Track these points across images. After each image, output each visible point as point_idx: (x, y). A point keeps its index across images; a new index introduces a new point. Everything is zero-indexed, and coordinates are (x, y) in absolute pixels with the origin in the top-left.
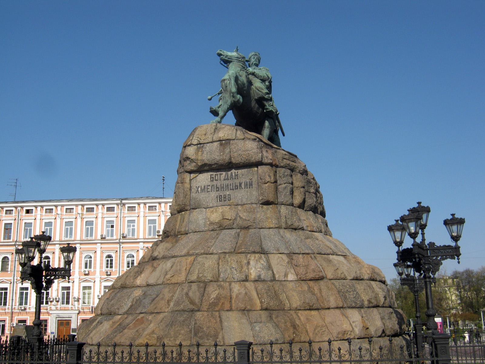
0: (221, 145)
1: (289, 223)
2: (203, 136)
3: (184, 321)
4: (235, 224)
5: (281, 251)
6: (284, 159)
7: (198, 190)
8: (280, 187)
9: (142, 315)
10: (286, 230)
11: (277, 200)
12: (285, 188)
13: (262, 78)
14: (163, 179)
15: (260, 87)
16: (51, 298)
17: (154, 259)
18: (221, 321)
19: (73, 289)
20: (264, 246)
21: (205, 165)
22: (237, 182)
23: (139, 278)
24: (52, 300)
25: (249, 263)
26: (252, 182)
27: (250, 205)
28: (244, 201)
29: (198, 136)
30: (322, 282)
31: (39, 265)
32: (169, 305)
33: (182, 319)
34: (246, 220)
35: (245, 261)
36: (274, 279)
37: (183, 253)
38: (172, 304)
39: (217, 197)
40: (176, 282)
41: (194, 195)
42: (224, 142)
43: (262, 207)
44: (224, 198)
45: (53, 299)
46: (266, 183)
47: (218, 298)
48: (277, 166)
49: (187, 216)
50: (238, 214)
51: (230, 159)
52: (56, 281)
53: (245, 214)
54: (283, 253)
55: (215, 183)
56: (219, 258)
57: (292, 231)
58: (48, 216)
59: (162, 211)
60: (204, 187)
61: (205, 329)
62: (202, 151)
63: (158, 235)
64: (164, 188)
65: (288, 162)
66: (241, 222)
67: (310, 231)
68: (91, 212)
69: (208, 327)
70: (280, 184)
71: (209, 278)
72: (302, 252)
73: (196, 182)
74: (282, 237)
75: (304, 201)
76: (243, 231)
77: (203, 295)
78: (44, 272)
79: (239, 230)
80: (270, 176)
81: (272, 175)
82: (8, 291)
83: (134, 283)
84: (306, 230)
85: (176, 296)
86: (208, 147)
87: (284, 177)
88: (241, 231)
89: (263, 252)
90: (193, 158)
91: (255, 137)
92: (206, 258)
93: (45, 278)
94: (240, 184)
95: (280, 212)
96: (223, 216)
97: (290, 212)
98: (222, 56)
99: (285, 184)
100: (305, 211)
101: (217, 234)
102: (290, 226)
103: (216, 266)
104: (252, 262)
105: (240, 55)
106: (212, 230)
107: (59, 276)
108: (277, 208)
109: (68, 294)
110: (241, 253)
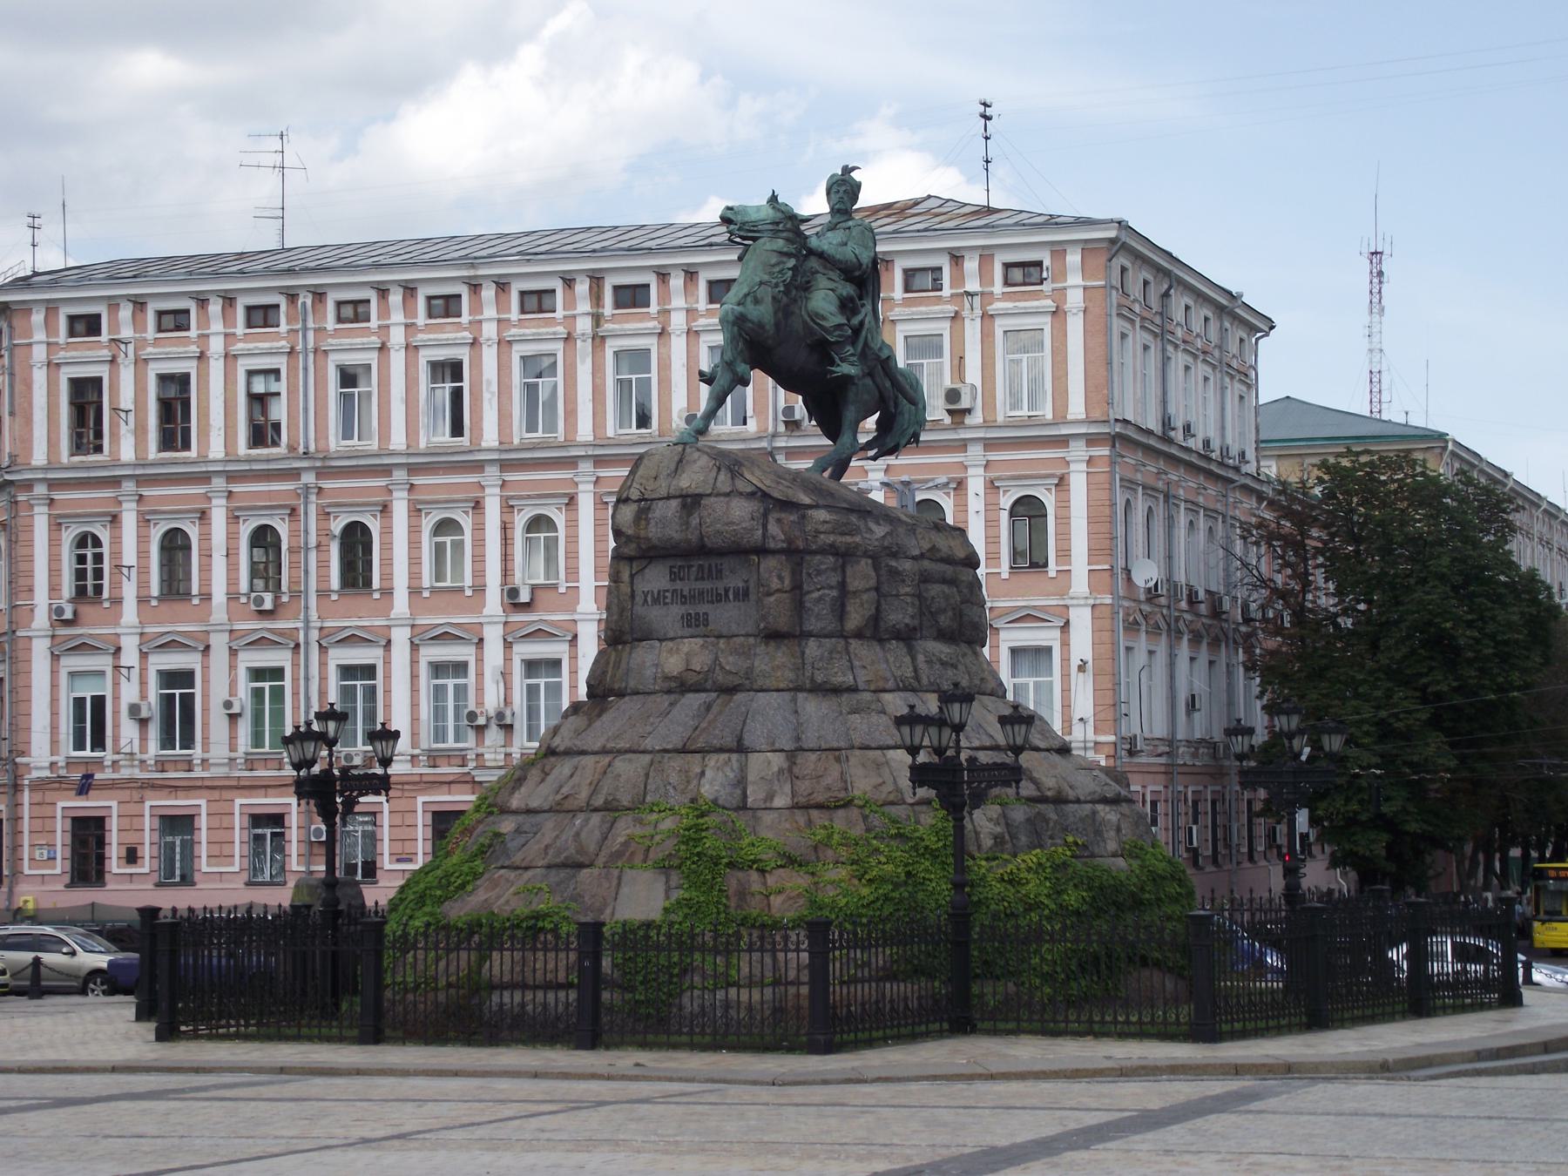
0: (684, 506)
1: (819, 678)
4: (710, 682)
5: (777, 746)
7: (646, 600)
10: (811, 697)
12: (820, 599)
13: (842, 266)
15: (817, 314)
16: (478, 711)
18: (619, 885)
20: (746, 736)
21: (654, 547)
22: (720, 586)
23: (517, 795)
24: (481, 721)
25: (703, 773)
27: (742, 639)
28: (734, 629)
30: (841, 813)
31: (327, 773)
32: (546, 854)
33: (557, 879)
35: (698, 770)
36: (743, 807)
37: (597, 746)
38: (551, 852)
39: (682, 617)
41: (639, 609)
42: (689, 500)
43: (767, 644)
45: (488, 719)
47: (626, 844)
48: (797, 551)
49: (625, 655)
50: (717, 658)
51: (702, 537)
53: (731, 659)
54: (782, 751)
55: (678, 585)
56: (652, 763)
58: (440, 327)
59: (971, 295)
61: (586, 899)
63: (950, 412)
64: (987, 162)
65: (832, 538)
66: (720, 678)
67: (875, 692)
68: (635, 306)
69: (593, 896)
70: (809, 592)
71: (625, 803)
72: (823, 746)
74: (796, 712)
75: (876, 619)
76: (724, 697)
77: (606, 838)
79: (714, 695)
80: (780, 578)
81: (787, 575)
82: (287, 683)
85: (564, 837)
87: (816, 575)
89: (741, 748)
90: (630, 532)
92: (630, 760)
94: (727, 591)
95: (803, 653)
96: (688, 662)
98: (732, 227)
99: (819, 590)
100: (881, 641)
101: (671, 704)
103: (642, 778)
104: (709, 774)
106: (669, 692)
108: (800, 645)
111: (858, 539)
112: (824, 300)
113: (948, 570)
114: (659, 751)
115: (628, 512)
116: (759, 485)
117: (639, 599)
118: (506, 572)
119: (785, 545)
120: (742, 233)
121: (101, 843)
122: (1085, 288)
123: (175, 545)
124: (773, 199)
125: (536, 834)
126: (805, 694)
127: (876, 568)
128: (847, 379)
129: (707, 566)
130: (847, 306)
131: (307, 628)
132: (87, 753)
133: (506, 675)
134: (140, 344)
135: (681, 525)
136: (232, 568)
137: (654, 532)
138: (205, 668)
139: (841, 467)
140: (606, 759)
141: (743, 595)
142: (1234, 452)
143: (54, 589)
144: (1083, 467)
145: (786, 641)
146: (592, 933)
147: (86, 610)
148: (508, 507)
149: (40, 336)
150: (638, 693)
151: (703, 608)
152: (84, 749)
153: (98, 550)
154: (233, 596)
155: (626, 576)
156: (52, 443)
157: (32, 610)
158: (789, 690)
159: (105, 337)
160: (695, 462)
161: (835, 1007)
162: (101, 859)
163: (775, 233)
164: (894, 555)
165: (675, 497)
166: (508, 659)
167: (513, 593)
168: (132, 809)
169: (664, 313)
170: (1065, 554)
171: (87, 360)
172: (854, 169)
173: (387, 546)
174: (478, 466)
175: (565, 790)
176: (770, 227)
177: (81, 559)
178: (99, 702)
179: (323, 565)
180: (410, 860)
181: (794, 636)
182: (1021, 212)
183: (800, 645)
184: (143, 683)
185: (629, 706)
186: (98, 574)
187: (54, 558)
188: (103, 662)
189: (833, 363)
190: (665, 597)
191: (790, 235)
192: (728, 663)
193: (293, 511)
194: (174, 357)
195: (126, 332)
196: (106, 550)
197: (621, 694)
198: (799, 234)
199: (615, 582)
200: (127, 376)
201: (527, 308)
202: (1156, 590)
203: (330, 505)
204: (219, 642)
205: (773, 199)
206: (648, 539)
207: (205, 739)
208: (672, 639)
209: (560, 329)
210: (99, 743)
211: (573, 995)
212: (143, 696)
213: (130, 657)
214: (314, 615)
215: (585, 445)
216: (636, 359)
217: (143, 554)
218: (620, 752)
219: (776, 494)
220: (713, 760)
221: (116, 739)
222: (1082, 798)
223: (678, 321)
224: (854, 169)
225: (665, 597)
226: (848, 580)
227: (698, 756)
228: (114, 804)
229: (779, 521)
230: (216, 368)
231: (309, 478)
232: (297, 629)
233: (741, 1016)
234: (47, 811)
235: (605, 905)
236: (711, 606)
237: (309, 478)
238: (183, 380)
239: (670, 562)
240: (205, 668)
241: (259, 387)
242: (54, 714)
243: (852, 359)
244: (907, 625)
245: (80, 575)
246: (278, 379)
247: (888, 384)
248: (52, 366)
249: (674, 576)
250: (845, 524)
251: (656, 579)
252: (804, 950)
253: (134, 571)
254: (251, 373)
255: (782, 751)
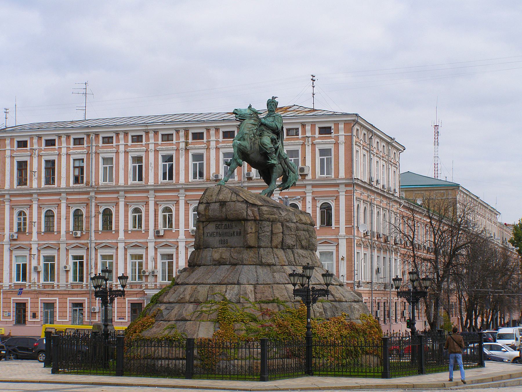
0: (220, 205)
2: (210, 197)
3: (179, 326)
5: (250, 283)
6: (265, 214)
7: (208, 235)
8: (260, 235)
9: (161, 322)
11: (257, 245)
12: (264, 236)
14: (312, 80)
17: (178, 284)
18: (199, 327)
19: (177, 258)
22: (231, 231)
24: (147, 274)
25: (226, 291)
26: (241, 231)
29: (206, 197)
34: (235, 259)
35: (225, 290)
36: (239, 302)
37: (192, 282)
40: (183, 302)
43: (247, 250)
44: (224, 242)
46: (248, 234)
50: (231, 254)
52: (116, 298)
53: (235, 254)
54: (252, 284)
55: (218, 230)
57: (265, 267)
60: (212, 232)
62: (208, 209)
64: (313, 94)
66: (231, 261)
67: (281, 266)
73: (207, 229)
78: (108, 293)
79: (229, 266)
80: (251, 229)
81: (253, 227)
83: (163, 300)
84: (278, 265)
86: (212, 206)
88: (231, 267)
89: (238, 284)
91: (243, 200)
93: (110, 297)
94: (234, 233)
95: (258, 253)
97: (266, 253)
98: (237, 116)
99: (264, 233)
100: (283, 249)
102: (264, 263)
103: (207, 293)
104: (228, 291)
105: (253, 111)
106: (215, 265)
107: (118, 295)
109: (170, 265)
110: (223, 284)
111: (277, 216)
112: (267, 140)
113: (305, 227)
114: (212, 284)
115: (202, 207)
116: (245, 199)
117: (205, 235)
118: (156, 225)
119: (253, 218)
120: (240, 118)
121: (25, 311)
122: (345, 136)
123: (49, 216)
124: (250, 107)
125: (172, 310)
126: (259, 266)
127: (282, 226)
128: (273, 165)
129: (227, 224)
130: (273, 141)
131: (91, 243)
132: (21, 282)
133: (155, 259)
134: (40, 150)
135: (220, 211)
136: (68, 223)
137: (211, 213)
138: (59, 255)
139: (271, 193)
140: (195, 286)
141: (239, 234)
142: (392, 189)
143: (11, 229)
144: (344, 193)
145: (253, 249)
146: (190, 342)
147: (21, 236)
148: (156, 204)
149: (8, 147)
150: (205, 265)
151: (226, 238)
152: (20, 281)
153: (24, 217)
154: (67, 232)
155: (201, 228)
156: (12, 182)
157: (4, 236)
158: (254, 265)
159: (29, 148)
160: (224, 191)
161: (269, 367)
162: (25, 316)
163: (251, 118)
164: (288, 221)
165: (218, 202)
166: (156, 254)
167: (158, 232)
168: (35, 300)
169: (209, 142)
170: (338, 222)
171: (23, 155)
172: (276, 98)
173: (117, 216)
174: (147, 191)
175: (181, 296)
176: (249, 116)
177: (20, 219)
178: (24, 266)
179: (97, 222)
180: (123, 319)
181: (256, 247)
182: (324, 111)
183: (257, 250)
184: (39, 260)
185: (202, 269)
186: (25, 224)
187: (11, 219)
188: (26, 253)
189: (269, 160)
190: (214, 234)
191: (256, 118)
192: (234, 256)
193: (87, 204)
194: (50, 154)
195: (35, 146)
196: (27, 217)
197: (199, 266)
198: (258, 118)
199: (198, 229)
200: (35, 160)
201: (164, 140)
202: (367, 234)
203: (99, 203)
204: (63, 247)
205: (250, 107)
206: (209, 215)
207: (58, 278)
208: (216, 248)
209: (174, 146)
210: (24, 279)
211: (185, 362)
212: (39, 264)
213: (34, 251)
214: (93, 238)
215: (182, 184)
216: (198, 157)
217: (39, 218)
218: (199, 284)
219: (250, 202)
220: (229, 287)
221: (30, 278)
222: (347, 301)
223: (213, 144)
224: (276, 98)
225: (214, 234)
226: (273, 229)
227: (225, 286)
228: (29, 299)
229: (251, 210)
230: (64, 159)
231: (92, 194)
232: (88, 243)
233: (239, 369)
234: (8, 300)
235: (195, 333)
236: (229, 237)
237: (92, 194)
238: (53, 162)
239: (216, 223)
240: (59, 255)
241: (77, 164)
242: (11, 269)
243: (275, 158)
244: (292, 244)
245: (19, 224)
246: (83, 162)
247: (286, 166)
248: (12, 157)
249: (217, 227)
250: (272, 212)
251: (211, 228)
252: (259, 348)
253: (36, 223)
254: (74, 160)
255: (252, 284)
